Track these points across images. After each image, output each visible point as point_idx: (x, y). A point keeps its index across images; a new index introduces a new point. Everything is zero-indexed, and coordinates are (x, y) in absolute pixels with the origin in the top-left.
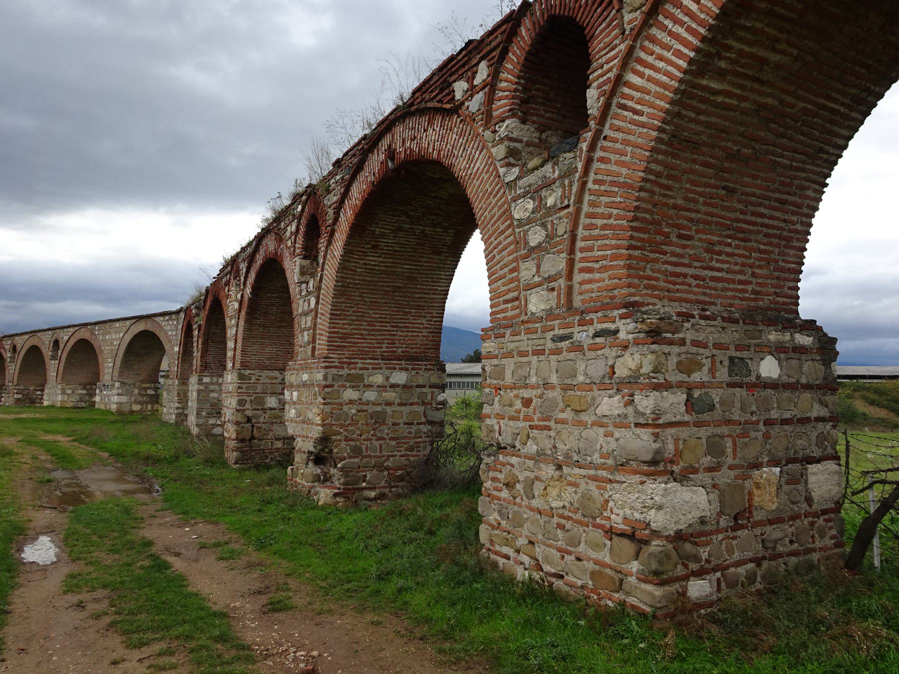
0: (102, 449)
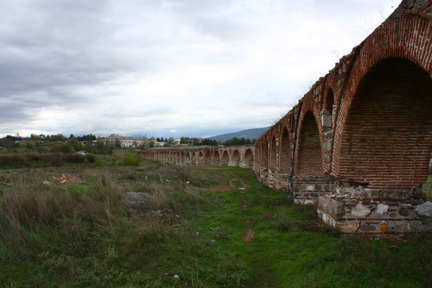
0: (239, 175)
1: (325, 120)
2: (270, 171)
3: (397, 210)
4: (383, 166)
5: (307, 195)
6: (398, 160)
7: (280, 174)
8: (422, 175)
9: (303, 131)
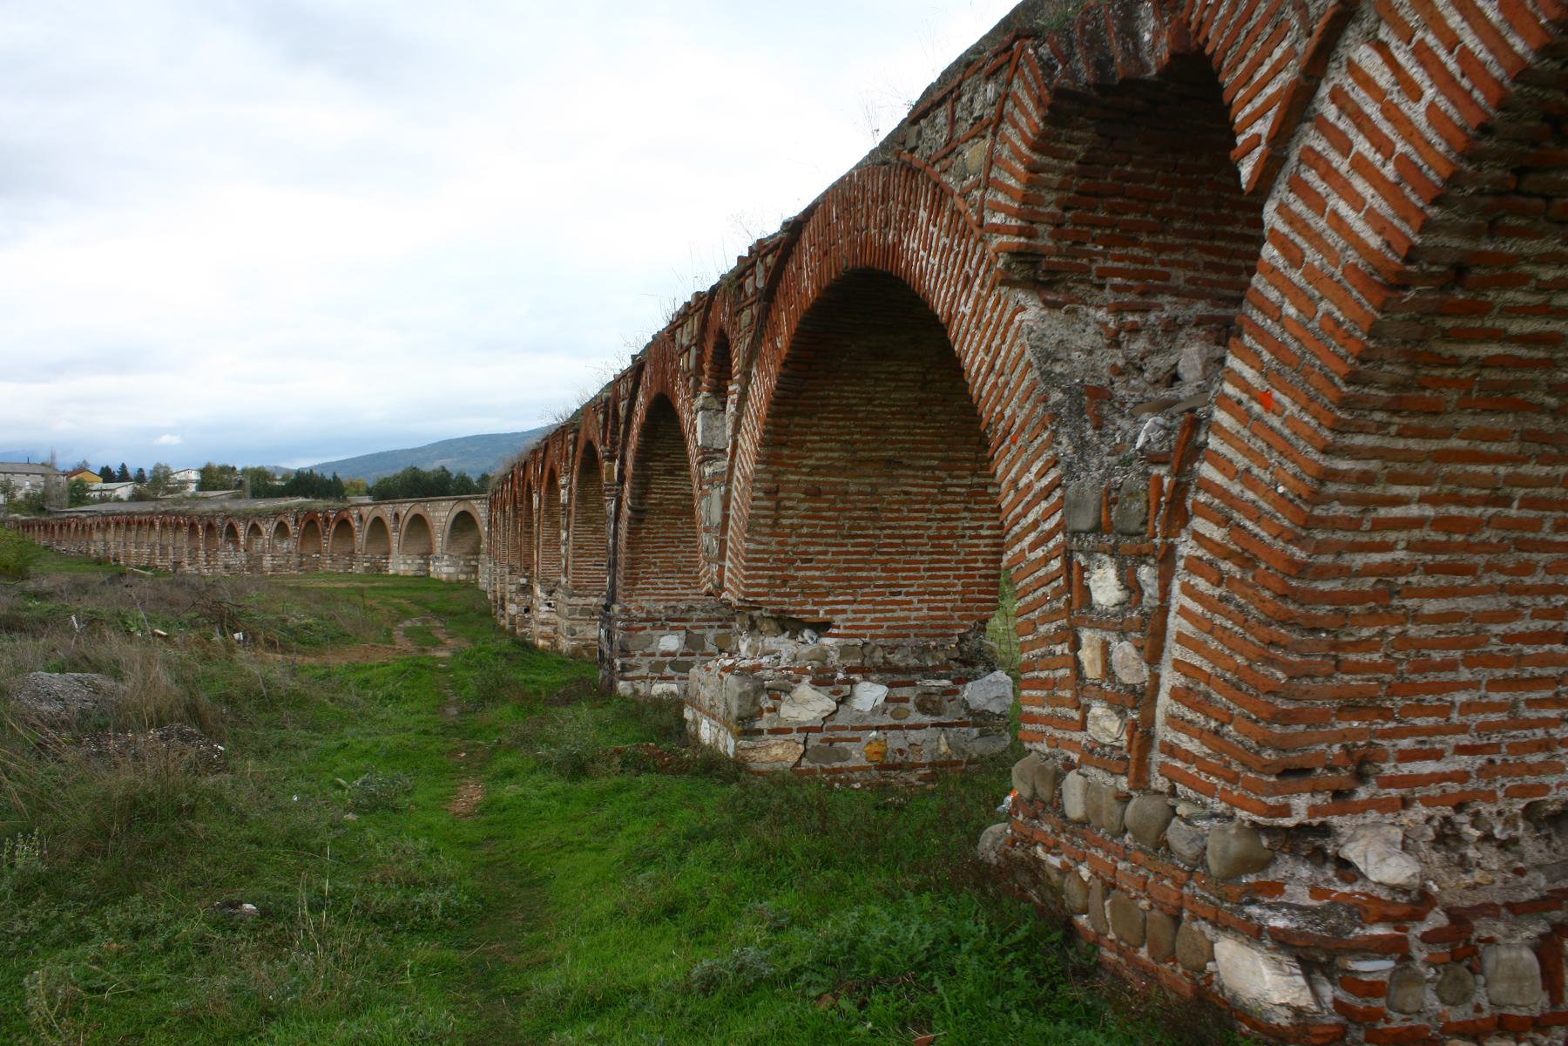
1: (707, 428)
2: (538, 590)
3: (912, 698)
4: (874, 569)
6: (914, 553)
7: (574, 600)
8: (983, 596)
9: (643, 457)
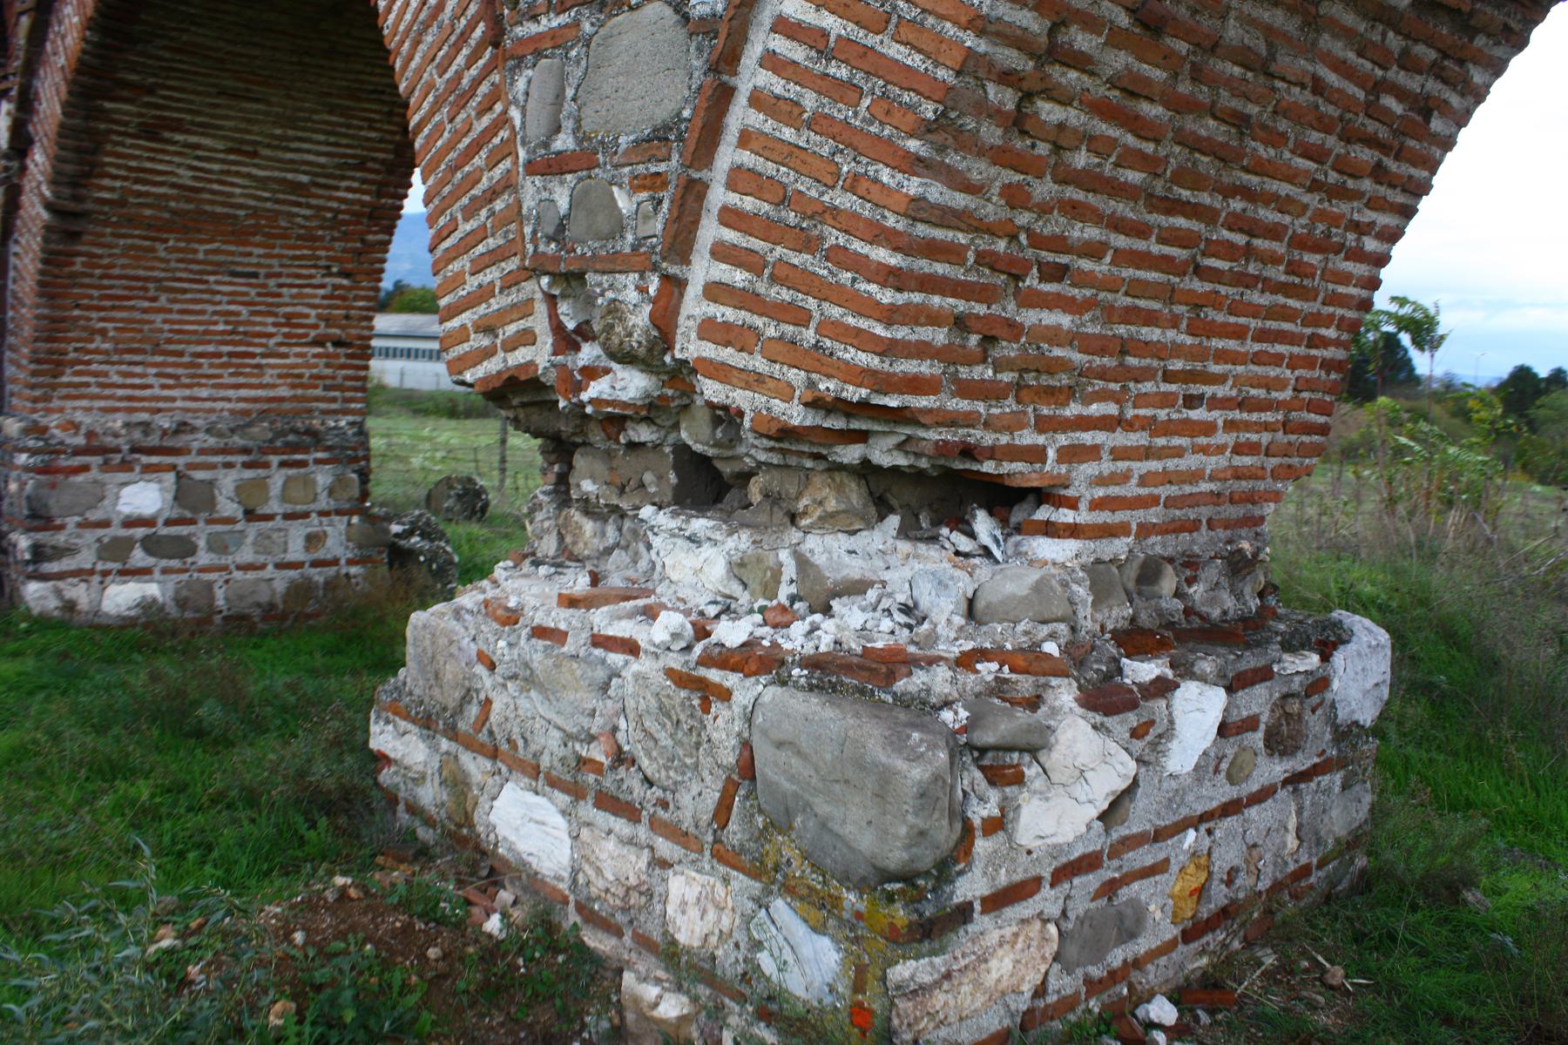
5: (115, 550)
